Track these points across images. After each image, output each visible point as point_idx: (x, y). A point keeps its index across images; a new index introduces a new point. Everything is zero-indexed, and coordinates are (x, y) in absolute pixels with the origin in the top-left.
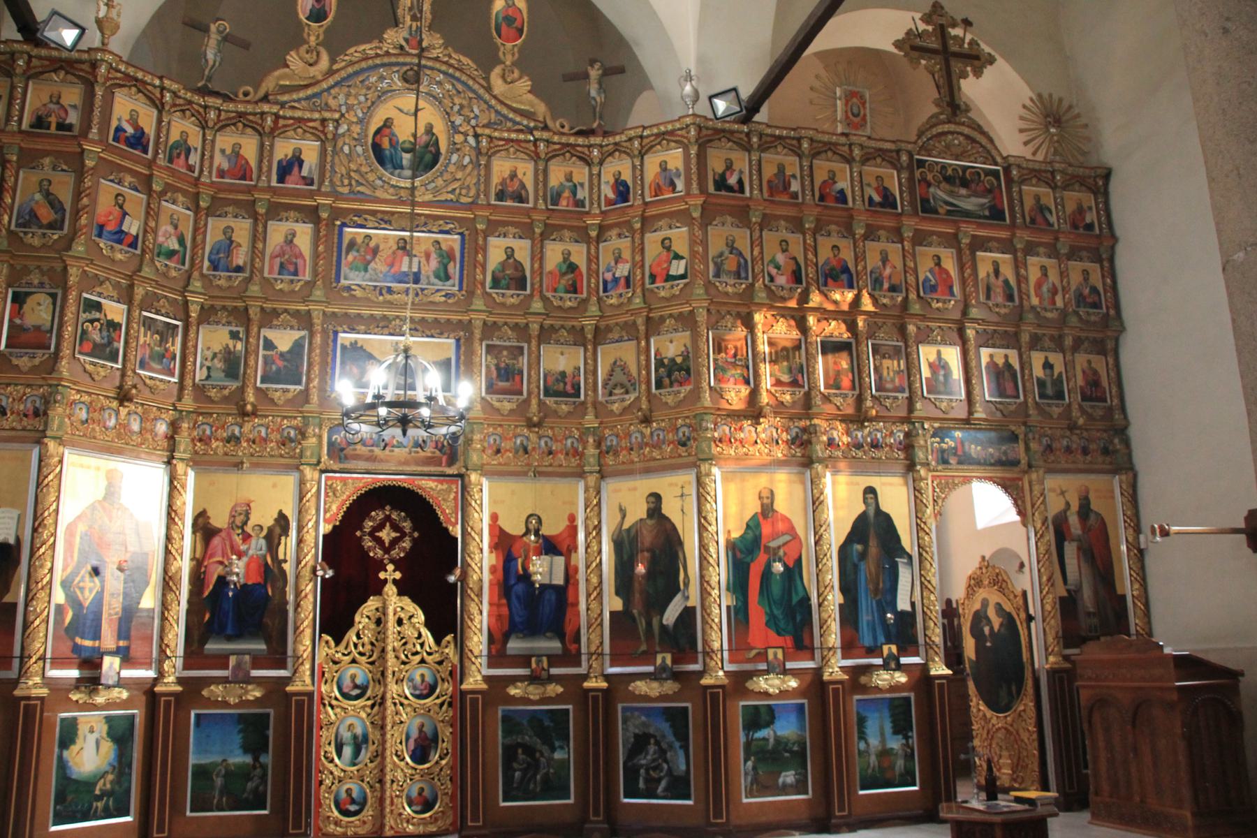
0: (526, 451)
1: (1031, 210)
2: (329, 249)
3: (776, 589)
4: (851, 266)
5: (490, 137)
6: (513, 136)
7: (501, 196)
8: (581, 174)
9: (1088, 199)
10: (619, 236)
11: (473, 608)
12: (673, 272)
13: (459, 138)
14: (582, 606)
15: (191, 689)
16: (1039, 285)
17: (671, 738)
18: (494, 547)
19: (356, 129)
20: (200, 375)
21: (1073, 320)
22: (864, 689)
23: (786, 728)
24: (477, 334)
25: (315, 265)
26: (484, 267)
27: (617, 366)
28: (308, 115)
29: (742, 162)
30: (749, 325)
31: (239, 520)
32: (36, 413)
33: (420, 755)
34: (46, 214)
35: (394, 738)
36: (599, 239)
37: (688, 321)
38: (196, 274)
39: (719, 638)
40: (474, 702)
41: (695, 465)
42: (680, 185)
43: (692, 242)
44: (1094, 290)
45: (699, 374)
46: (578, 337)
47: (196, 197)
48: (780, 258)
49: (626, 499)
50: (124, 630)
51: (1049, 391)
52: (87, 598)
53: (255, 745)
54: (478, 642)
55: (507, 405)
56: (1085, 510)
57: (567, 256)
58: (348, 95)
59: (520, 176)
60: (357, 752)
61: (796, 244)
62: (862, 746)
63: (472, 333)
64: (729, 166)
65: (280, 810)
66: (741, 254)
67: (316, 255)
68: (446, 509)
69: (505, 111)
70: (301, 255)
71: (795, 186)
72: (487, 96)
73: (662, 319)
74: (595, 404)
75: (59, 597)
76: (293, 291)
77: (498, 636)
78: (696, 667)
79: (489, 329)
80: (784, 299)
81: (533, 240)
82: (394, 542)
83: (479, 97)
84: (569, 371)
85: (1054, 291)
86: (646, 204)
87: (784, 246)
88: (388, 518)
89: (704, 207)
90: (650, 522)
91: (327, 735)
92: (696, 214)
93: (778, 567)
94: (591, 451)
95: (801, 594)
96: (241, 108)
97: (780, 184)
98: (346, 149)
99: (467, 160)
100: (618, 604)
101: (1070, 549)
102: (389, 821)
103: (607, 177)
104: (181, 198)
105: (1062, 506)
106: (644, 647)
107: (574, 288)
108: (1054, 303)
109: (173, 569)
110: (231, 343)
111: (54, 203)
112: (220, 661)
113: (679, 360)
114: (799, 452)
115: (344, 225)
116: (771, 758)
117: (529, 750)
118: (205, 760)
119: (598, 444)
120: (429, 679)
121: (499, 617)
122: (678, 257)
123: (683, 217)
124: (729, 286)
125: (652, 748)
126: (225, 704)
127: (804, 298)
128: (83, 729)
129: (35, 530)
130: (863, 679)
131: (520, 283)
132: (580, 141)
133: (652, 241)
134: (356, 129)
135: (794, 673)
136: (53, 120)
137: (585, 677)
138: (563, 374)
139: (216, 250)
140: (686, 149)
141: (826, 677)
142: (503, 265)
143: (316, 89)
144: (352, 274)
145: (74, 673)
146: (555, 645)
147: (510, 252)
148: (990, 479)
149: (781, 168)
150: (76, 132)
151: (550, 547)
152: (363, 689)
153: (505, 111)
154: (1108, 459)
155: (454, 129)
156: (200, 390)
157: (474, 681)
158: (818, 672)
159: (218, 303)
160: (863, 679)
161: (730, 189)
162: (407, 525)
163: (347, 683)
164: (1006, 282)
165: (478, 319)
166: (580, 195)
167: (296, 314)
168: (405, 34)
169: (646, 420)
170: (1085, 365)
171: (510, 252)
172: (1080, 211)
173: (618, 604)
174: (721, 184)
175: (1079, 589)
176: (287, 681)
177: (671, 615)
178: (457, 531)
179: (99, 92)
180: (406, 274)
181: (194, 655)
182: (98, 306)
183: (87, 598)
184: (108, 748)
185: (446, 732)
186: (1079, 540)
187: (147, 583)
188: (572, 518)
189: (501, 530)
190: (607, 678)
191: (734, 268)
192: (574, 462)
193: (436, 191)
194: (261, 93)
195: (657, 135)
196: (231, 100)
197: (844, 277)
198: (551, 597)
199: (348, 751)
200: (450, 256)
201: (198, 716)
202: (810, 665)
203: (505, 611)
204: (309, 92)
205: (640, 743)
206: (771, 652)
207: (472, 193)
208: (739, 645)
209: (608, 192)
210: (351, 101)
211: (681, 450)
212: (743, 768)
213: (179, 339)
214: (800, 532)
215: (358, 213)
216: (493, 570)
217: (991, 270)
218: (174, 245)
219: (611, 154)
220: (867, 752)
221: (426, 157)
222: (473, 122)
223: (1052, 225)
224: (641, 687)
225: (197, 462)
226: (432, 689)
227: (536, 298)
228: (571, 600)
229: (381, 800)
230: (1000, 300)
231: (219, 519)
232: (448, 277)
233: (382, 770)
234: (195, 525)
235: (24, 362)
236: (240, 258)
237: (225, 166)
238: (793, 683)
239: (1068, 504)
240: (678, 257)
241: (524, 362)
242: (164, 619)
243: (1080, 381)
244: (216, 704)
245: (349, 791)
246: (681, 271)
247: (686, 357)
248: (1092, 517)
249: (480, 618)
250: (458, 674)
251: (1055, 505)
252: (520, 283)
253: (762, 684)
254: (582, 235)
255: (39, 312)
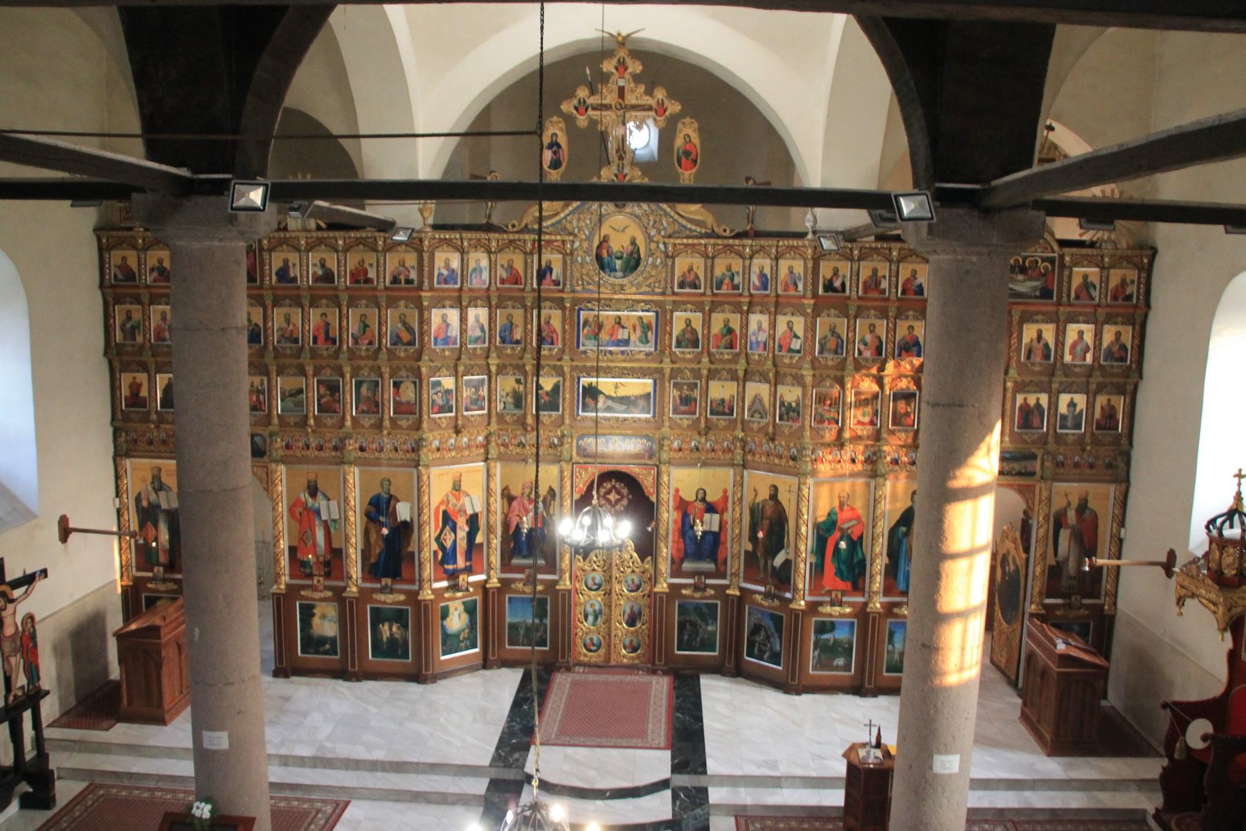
0: (697, 449)
1: (1079, 287)
2: (571, 325)
3: (844, 555)
4: (921, 341)
5: (675, 245)
6: (690, 241)
7: (681, 285)
8: (737, 264)
9: (1132, 274)
10: (761, 312)
11: (662, 545)
12: (792, 347)
13: (653, 246)
14: (729, 545)
15: (506, 584)
16: (1074, 346)
17: (773, 630)
18: (677, 508)
19: (585, 245)
20: (500, 407)
21: (1097, 373)
22: (896, 616)
23: (841, 635)
24: (667, 376)
25: (564, 338)
26: (671, 335)
27: (757, 399)
28: (553, 238)
29: (845, 268)
30: (843, 386)
31: (527, 491)
32: (413, 450)
33: (631, 622)
34: (406, 336)
35: (616, 613)
36: (748, 312)
37: (799, 380)
38: (493, 348)
39: (802, 580)
40: (661, 599)
41: (797, 474)
42: (800, 287)
43: (806, 330)
44: (1124, 347)
45: (804, 419)
46: (733, 376)
47: (488, 299)
48: (868, 337)
49: (759, 483)
50: (468, 556)
51: (1069, 423)
52: (448, 544)
53: (541, 612)
54: (664, 567)
55: (685, 421)
56: (1083, 507)
57: (726, 323)
58: (579, 220)
59: (695, 268)
60: (596, 619)
61: (882, 327)
62: (890, 647)
63: (664, 376)
64: (836, 273)
65: (554, 647)
66: (839, 337)
67: (564, 331)
68: (648, 483)
69: (684, 223)
70: (554, 331)
71: (884, 284)
72: (672, 213)
73: (785, 375)
74: (743, 421)
75: (435, 546)
76: (551, 356)
77: (677, 560)
78: (788, 595)
79: (674, 373)
80: (868, 368)
81: (704, 313)
82: (617, 501)
83: (666, 214)
84: (727, 398)
85: (1087, 349)
86: (777, 296)
87: (872, 328)
88: (614, 487)
89: (815, 305)
90: (771, 503)
91: (579, 609)
92: (809, 311)
93: (843, 545)
94: (739, 451)
95: (860, 556)
96: (511, 237)
97: (873, 283)
98: (579, 259)
99: (659, 261)
100: (750, 547)
101: (1064, 535)
102: (613, 656)
103: (755, 270)
104: (479, 302)
105: (1064, 504)
106: (762, 575)
107: (731, 346)
108: (1084, 359)
109: (492, 521)
110: (516, 386)
111: (410, 330)
112: (520, 569)
113: (794, 405)
114: (869, 467)
115: (580, 309)
116: (829, 651)
117: (694, 625)
118: (515, 620)
119: (743, 448)
120: (637, 581)
121: (678, 550)
122: (797, 337)
123: (799, 310)
124: (830, 359)
125: (763, 633)
126: (524, 592)
127: (882, 369)
128: (451, 609)
129: (419, 515)
130: (896, 610)
131: (695, 343)
132: (737, 242)
133: (782, 321)
134: (585, 245)
135: (850, 604)
136: (402, 278)
137: (728, 587)
138: (723, 401)
139: (503, 330)
140: (805, 260)
141: (868, 610)
142: (684, 331)
143: (558, 218)
144: (587, 343)
145: (445, 584)
146: (710, 566)
147: (688, 322)
148: (1010, 486)
149: (875, 271)
150: (416, 284)
151: (711, 508)
152: (600, 586)
153: (684, 223)
154: (1110, 472)
155: (650, 239)
156: (501, 417)
157: (662, 587)
158: (865, 604)
159: (507, 363)
160: (896, 610)
161: (835, 290)
162: (625, 491)
163: (590, 583)
164: (1046, 345)
165: (667, 366)
166: (736, 281)
167: (554, 368)
168: (614, 169)
169: (772, 439)
170: (1105, 403)
171: (688, 322)
172: (1123, 283)
173: (750, 547)
174: (829, 287)
175: (1067, 559)
176: (556, 582)
177: (779, 560)
178: (653, 498)
179: (426, 256)
180: (620, 341)
181: (506, 566)
182: (439, 384)
183: (448, 544)
184: (465, 617)
185: (646, 611)
186: (1073, 528)
187: (478, 529)
188: (725, 491)
189: (681, 499)
190: (741, 589)
191: (833, 347)
192: (729, 456)
193: (639, 286)
194: (523, 225)
195: (788, 247)
196: (505, 232)
197: (915, 349)
198: (710, 538)
199: (591, 618)
200: (649, 327)
201: (510, 599)
202: (860, 599)
203: (682, 546)
204: (554, 220)
205: (756, 629)
206: (834, 594)
207: (663, 284)
208: (816, 587)
209: (755, 279)
210: (582, 224)
211: (791, 463)
212: (812, 655)
213: (486, 387)
214: (864, 519)
215: (589, 301)
216: (675, 522)
217: (1035, 336)
218: (478, 333)
219: (757, 252)
220: (893, 652)
221: (633, 263)
222: (663, 233)
223: (1093, 299)
224: (758, 597)
225: (501, 458)
226: (638, 587)
227: (705, 355)
228: (722, 539)
229: (609, 645)
230: (1037, 358)
231: (516, 491)
232: (647, 342)
233: (610, 629)
234: (502, 494)
235: (404, 423)
236: (518, 335)
237: (505, 275)
238: (848, 610)
239: (1069, 503)
240: (798, 337)
241: (696, 394)
242: (489, 547)
243: (1098, 415)
244: (519, 592)
245: (591, 639)
246: (798, 347)
247: (798, 405)
248: (1087, 512)
249: (666, 551)
250: (654, 580)
251: (1058, 504)
252: (695, 343)
253: (828, 609)
254: (737, 308)
255: (408, 393)
